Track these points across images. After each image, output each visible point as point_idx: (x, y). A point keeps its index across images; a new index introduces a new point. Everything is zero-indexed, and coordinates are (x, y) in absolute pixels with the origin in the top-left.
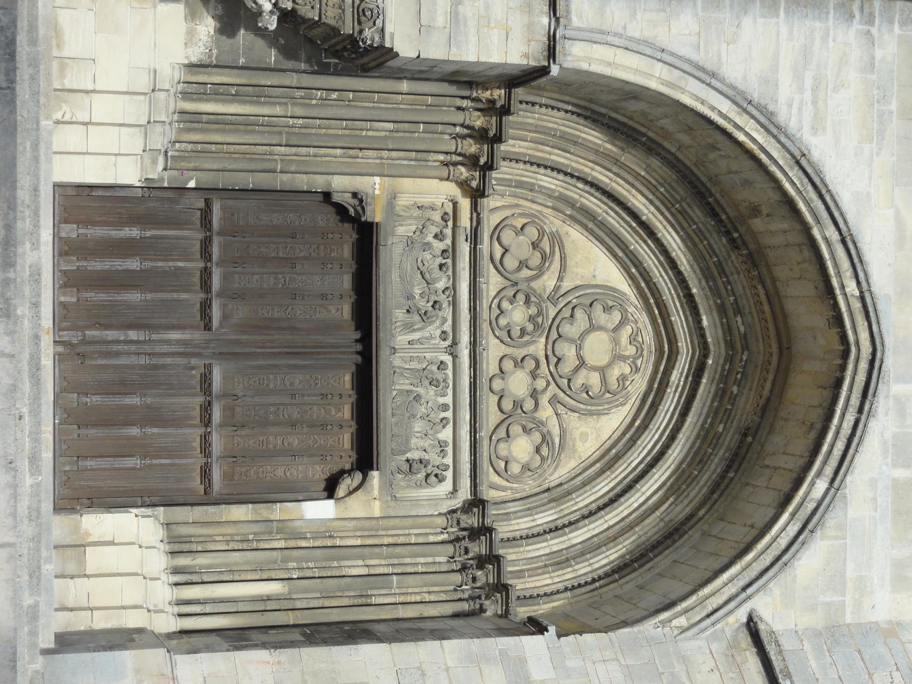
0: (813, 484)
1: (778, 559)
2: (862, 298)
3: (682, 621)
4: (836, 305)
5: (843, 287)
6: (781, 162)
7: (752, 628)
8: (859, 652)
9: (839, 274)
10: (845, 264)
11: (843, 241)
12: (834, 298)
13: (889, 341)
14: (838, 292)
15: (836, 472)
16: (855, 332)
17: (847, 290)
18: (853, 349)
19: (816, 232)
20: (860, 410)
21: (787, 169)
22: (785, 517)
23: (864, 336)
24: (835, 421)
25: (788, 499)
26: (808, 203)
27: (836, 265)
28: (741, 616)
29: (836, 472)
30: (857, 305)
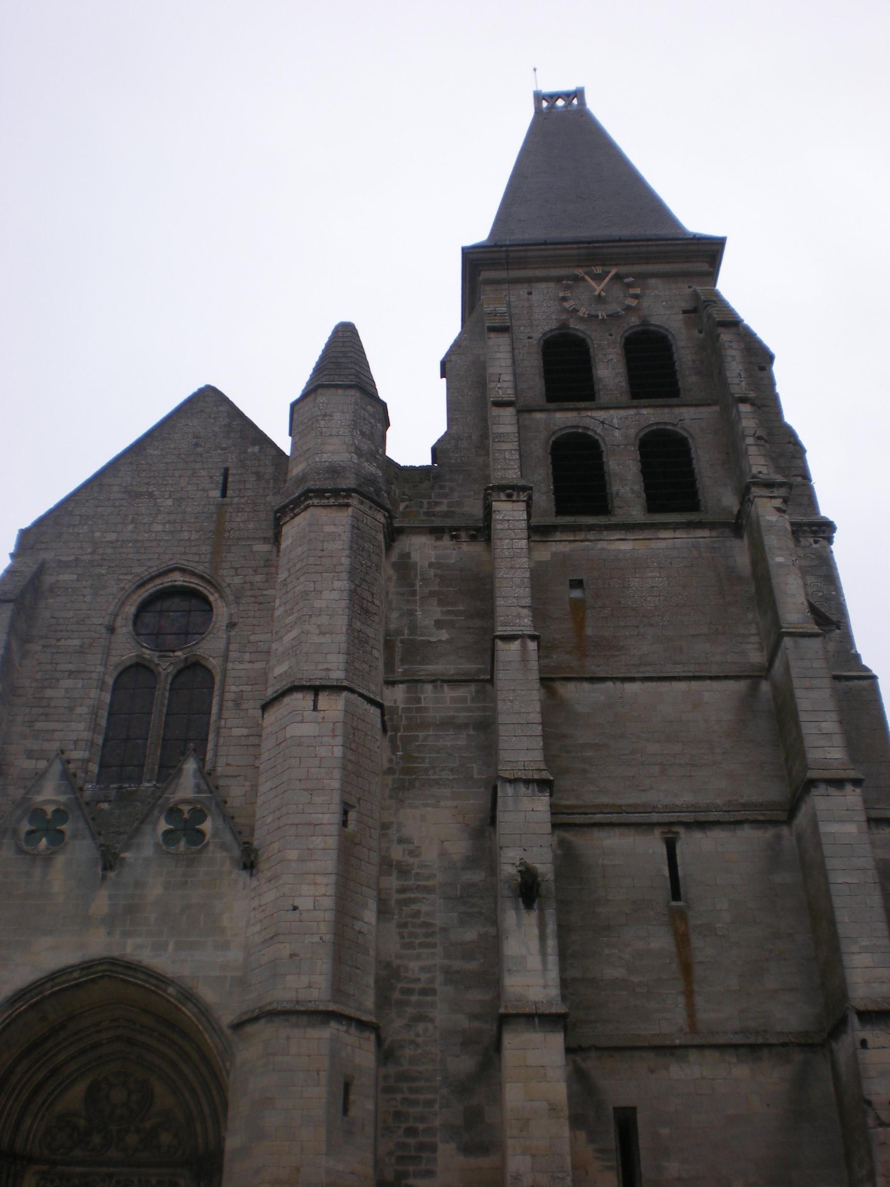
0: (170, 995)
1: (203, 1014)
2: (83, 969)
3: (228, 1064)
4: (85, 982)
5: (75, 979)
6: (10, 1012)
7: (237, 1026)
8: (252, 970)
9: (68, 981)
10: (64, 978)
11: (53, 979)
12: (81, 983)
13: (105, 954)
14: (77, 981)
15: (164, 982)
16: (98, 972)
17: (77, 976)
18: (106, 973)
19: (47, 993)
20: (135, 970)
21: (14, 1009)
22: (184, 1009)
23: (100, 968)
24: (140, 982)
25: (176, 1006)
26: (32, 998)
27: (64, 982)
28: (228, 1032)
29: (164, 982)
30: (85, 972)
